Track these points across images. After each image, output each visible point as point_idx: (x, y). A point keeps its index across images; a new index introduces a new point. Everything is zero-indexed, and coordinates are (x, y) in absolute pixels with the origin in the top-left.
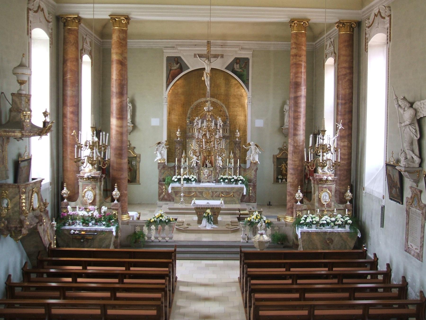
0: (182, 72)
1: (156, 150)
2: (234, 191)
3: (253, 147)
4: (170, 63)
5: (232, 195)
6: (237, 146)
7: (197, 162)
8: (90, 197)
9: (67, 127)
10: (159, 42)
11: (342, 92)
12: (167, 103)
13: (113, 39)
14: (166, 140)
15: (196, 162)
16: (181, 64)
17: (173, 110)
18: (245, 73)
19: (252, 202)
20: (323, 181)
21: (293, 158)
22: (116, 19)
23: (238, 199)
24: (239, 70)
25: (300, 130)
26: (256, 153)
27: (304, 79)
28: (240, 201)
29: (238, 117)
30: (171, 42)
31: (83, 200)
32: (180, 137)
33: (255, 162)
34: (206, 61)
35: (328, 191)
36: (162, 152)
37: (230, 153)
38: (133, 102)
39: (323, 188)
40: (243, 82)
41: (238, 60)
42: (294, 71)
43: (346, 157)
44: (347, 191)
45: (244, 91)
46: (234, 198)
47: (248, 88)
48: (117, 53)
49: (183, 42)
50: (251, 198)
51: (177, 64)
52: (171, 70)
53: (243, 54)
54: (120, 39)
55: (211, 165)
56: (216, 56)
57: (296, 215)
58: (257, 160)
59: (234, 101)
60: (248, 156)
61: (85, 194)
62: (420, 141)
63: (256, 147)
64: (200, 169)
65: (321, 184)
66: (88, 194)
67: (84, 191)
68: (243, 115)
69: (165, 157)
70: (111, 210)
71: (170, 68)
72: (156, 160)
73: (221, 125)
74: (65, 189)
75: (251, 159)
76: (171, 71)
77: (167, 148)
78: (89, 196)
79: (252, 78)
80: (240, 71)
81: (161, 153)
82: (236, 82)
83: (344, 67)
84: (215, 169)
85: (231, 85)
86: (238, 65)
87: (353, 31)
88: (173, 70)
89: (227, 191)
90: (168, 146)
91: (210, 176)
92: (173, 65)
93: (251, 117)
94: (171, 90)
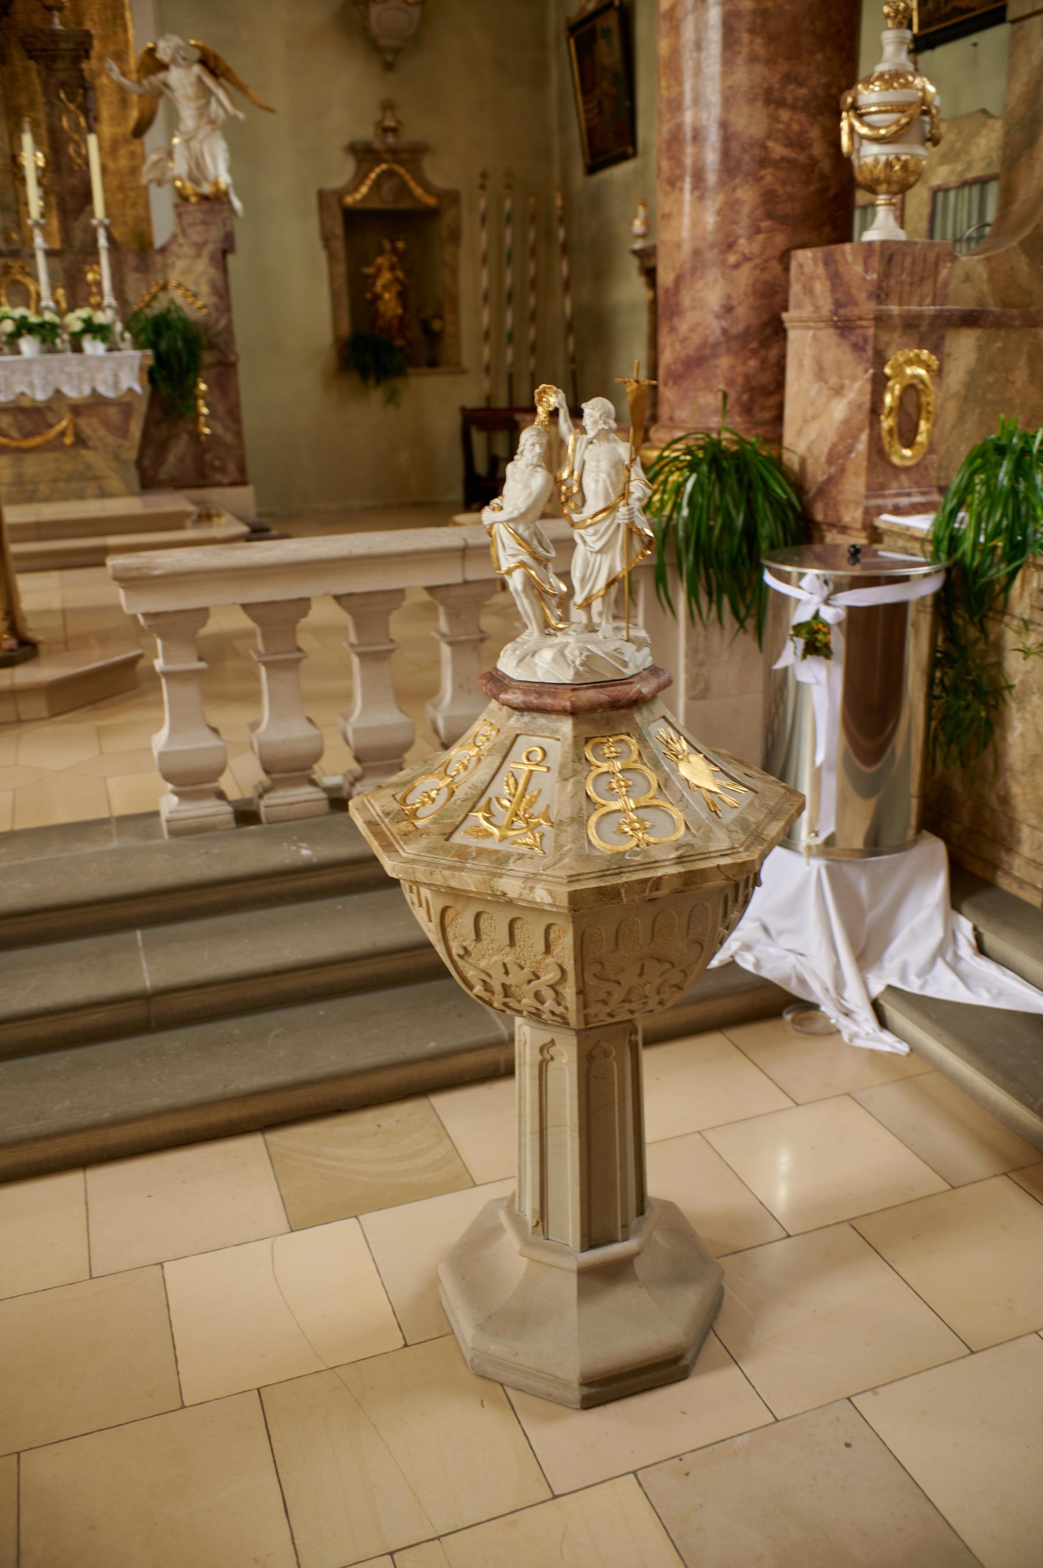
5: (62, 434)
6: (61, 76)
19: (220, 485)
23: (117, 458)
26: (212, 122)
28: (133, 475)
33: (207, 189)
46: (84, 452)
50: (208, 457)
58: (225, 179)
63: (209, 81)
75: (180, 166)
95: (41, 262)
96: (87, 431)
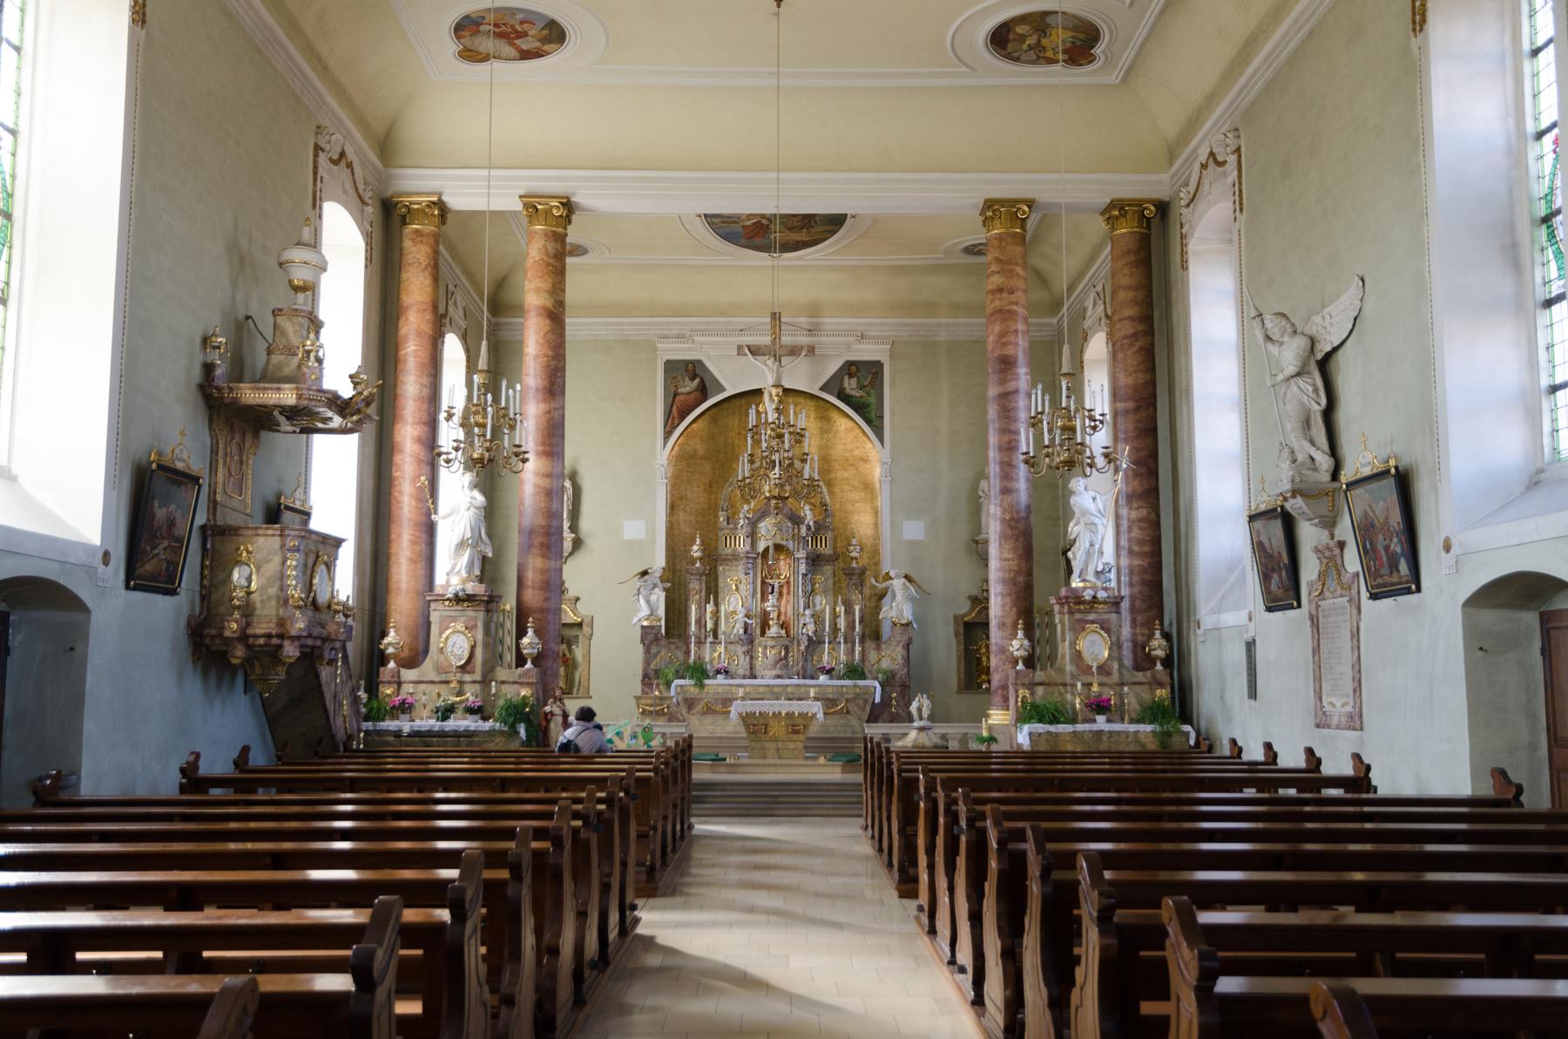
0: (705, 399)
2: (847, 696)
3: (898, 584)
4: (674, 378)
7: (745, 623)
10: (645, 324)
11: (1125, 380)
13: (531, 255)
14: (663, 564)
15: (745, 623)
16: (702, 379)
17: (682, 498)
18: (873, 400)
20: (1084, 602)
21: (1001, 553)
22: (539, 207)
24: (858, 393)
25: (1017, 480)
27: (1025, 349)
29: (856, 517)
30: (677, 323)
31: (442, 658)
32: (701, 559)
33: (904, 622)
34: (770, 362)
35: (1102, 632)
36: (653, 598)
37: (835, 603)
38: (573, 477)
39: (1086, 622)
40: (869, 422)
41: (854, 367)
42: (997, 328)
43: (1147, 548)
44: (1154, 635)
45: (871, 446)
47: (882, 442)
48: (538, 290)
49: (708, 323)
51: (692, 379)
52: (676, 395)
53: (866, 352)
54: (548, 255)
55: (783, 632)
56: (794, 351)
57: (1017, 697)
59: (846, 474)
60: (884, 609)
62: (1329, 414)
63: (908, 584)
64: (757, 642)
65: (1080, 611)
67: (444, 636)
68: (869, 510)
69: (661, 612)
70: (516, 686)
72: (635, 620)
73: (811, 523)
74: (392, 633)
77: (665, 590)
79: (892, 413)
80: (858, 395)
81: (648, 602)
82: (850, 424)
83: (1129, 318)
84: (795, 643)
85: (836, 432)
86: (854, 381)
87: (1149, 227)
88: (682, 394)
89: (830, 696)
90: (669, 585)
91: (781, 660)
93: (892, 513)
94: (676, 447)
95: (842, 646)
96: (850, 708)
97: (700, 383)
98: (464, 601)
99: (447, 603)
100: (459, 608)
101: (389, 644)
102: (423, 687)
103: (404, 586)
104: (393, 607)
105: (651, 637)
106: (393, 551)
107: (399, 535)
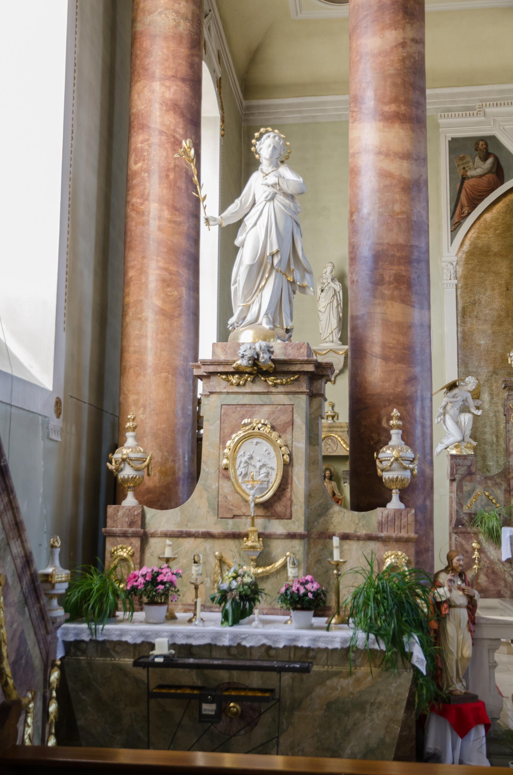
1: (441, 411)
4: (462, 159)
8: (264, 470)
9: (148, 171)
12: (456, 278)
17: (474, 303)
51: (484, 159)
52: (464, 179)
61: (234, 459)
66: (251, 458)
71: (460, 172)
74: (130, 440)
76: (466, 182)
78: (258, 465)
88: (472, 177)
92: (471, 164)
94: (467, 243)
97: (493, 164)
98: (266, 374)
99: (234, 379)
100: (258, 388)
101: (124, 460)
102: (188, 543)
103: (150, 359)
104: (132, 398)
105: (462, 470)
106: (131, 299)
107: (142, 271)
